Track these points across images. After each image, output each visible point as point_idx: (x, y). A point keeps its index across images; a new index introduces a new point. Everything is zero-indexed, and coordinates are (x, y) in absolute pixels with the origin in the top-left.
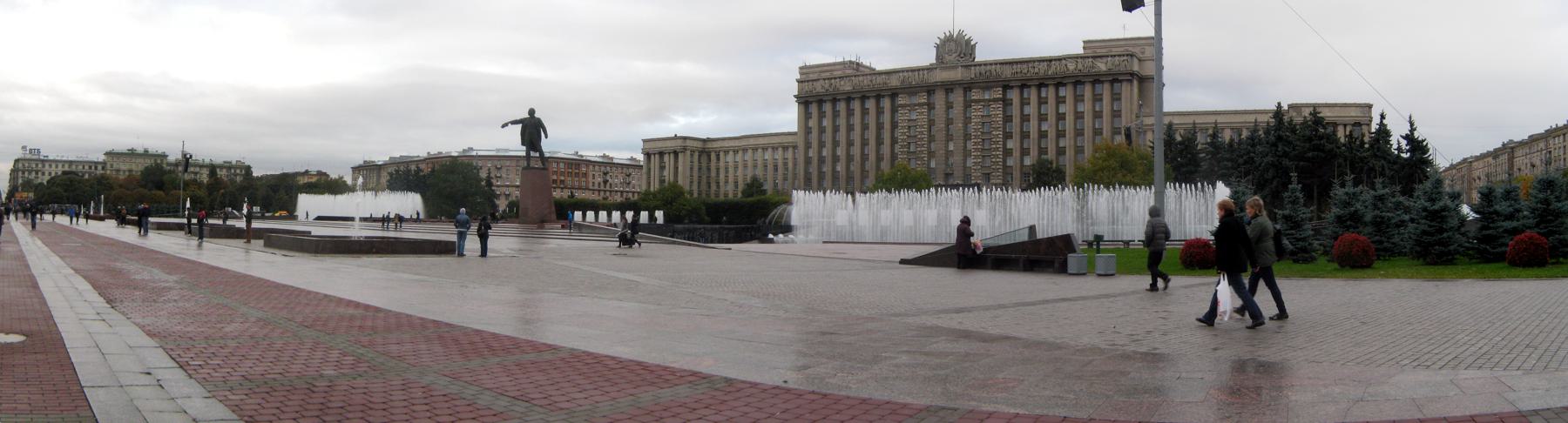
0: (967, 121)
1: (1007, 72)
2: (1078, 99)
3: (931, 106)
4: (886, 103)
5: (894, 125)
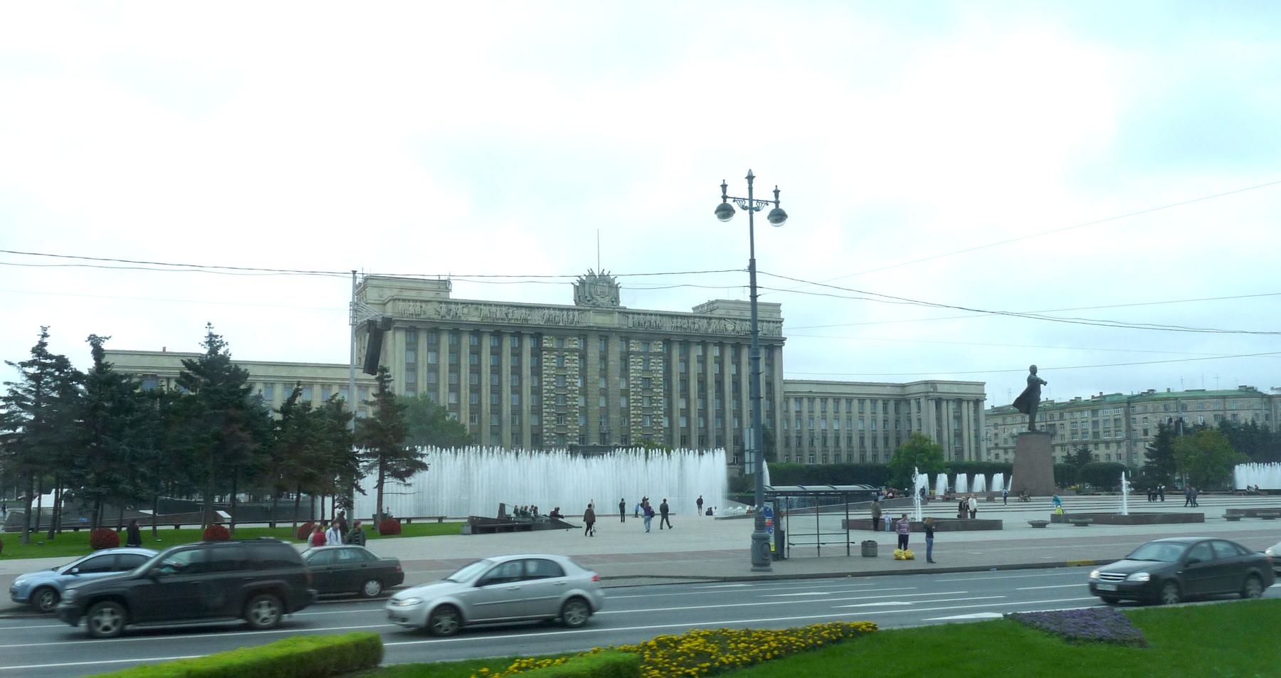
1: (668, 326)
4: (528, 344)
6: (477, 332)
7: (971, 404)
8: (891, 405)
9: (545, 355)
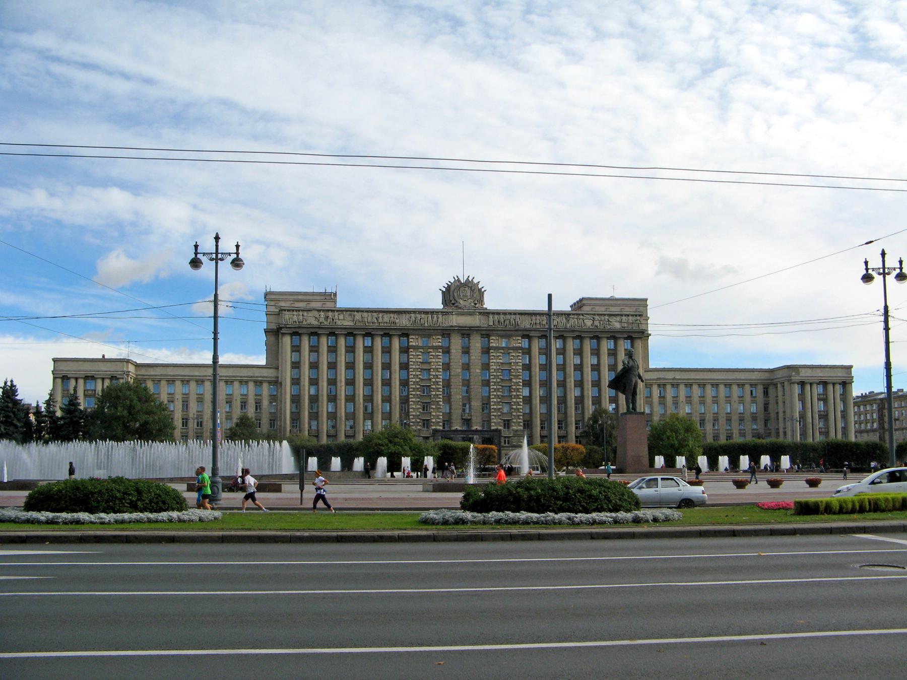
0: (486, 367)
1: (526, 323)
2: (596, 352)
3: (447, 351)
5: (404, 366)
6: (350, 333)
7: (838, 387)
8: (760, 389)
9: (412, 352)
